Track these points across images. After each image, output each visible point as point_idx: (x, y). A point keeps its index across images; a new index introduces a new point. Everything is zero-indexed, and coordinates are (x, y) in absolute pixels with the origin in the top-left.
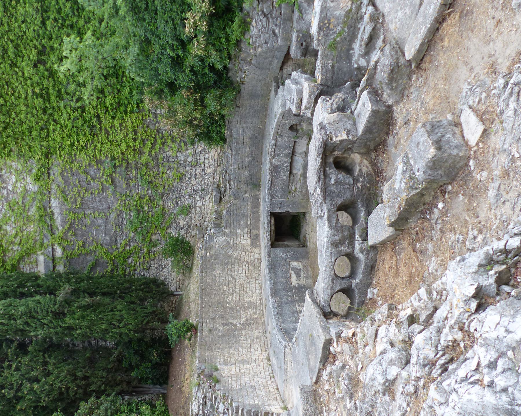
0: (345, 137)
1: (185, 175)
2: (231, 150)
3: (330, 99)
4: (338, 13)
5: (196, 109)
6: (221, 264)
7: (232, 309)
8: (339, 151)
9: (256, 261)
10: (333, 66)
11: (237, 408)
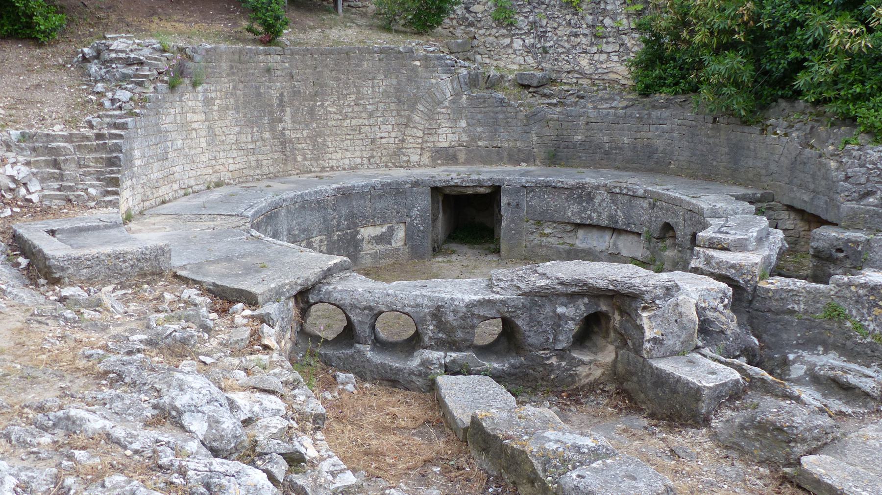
0: (648, 334)
1: (575, 14)
2: (626, 107)
3: (725, 306)
5: (712, 33)
6: (398, 90)
7: (312, 111)
8: (621, 322)
9: (406, 158)
10: (792, 312)
11: (124, 126)
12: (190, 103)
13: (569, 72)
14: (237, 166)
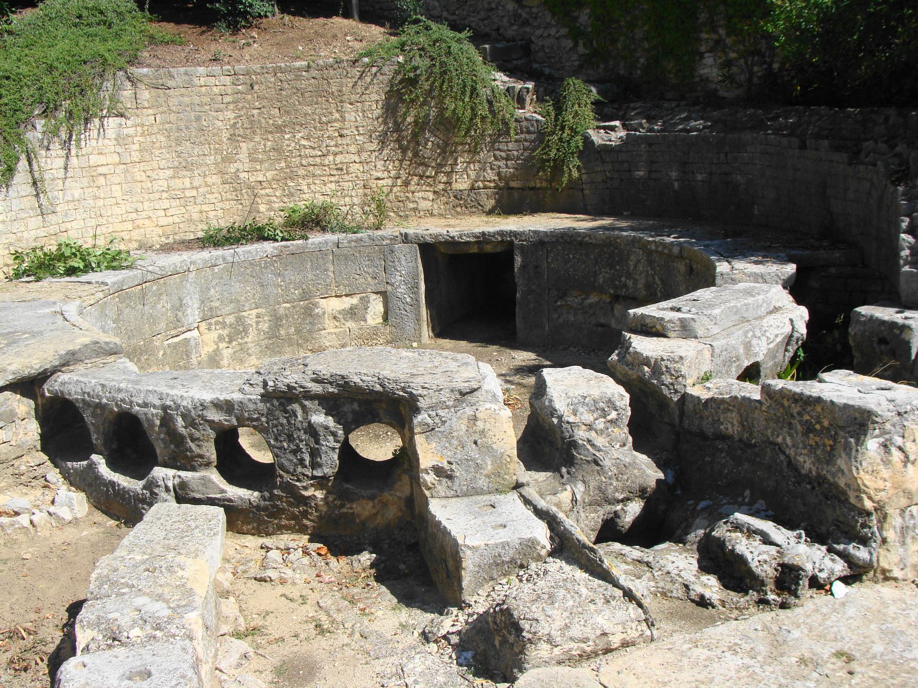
9: (412, 205)
14: (170, 220)
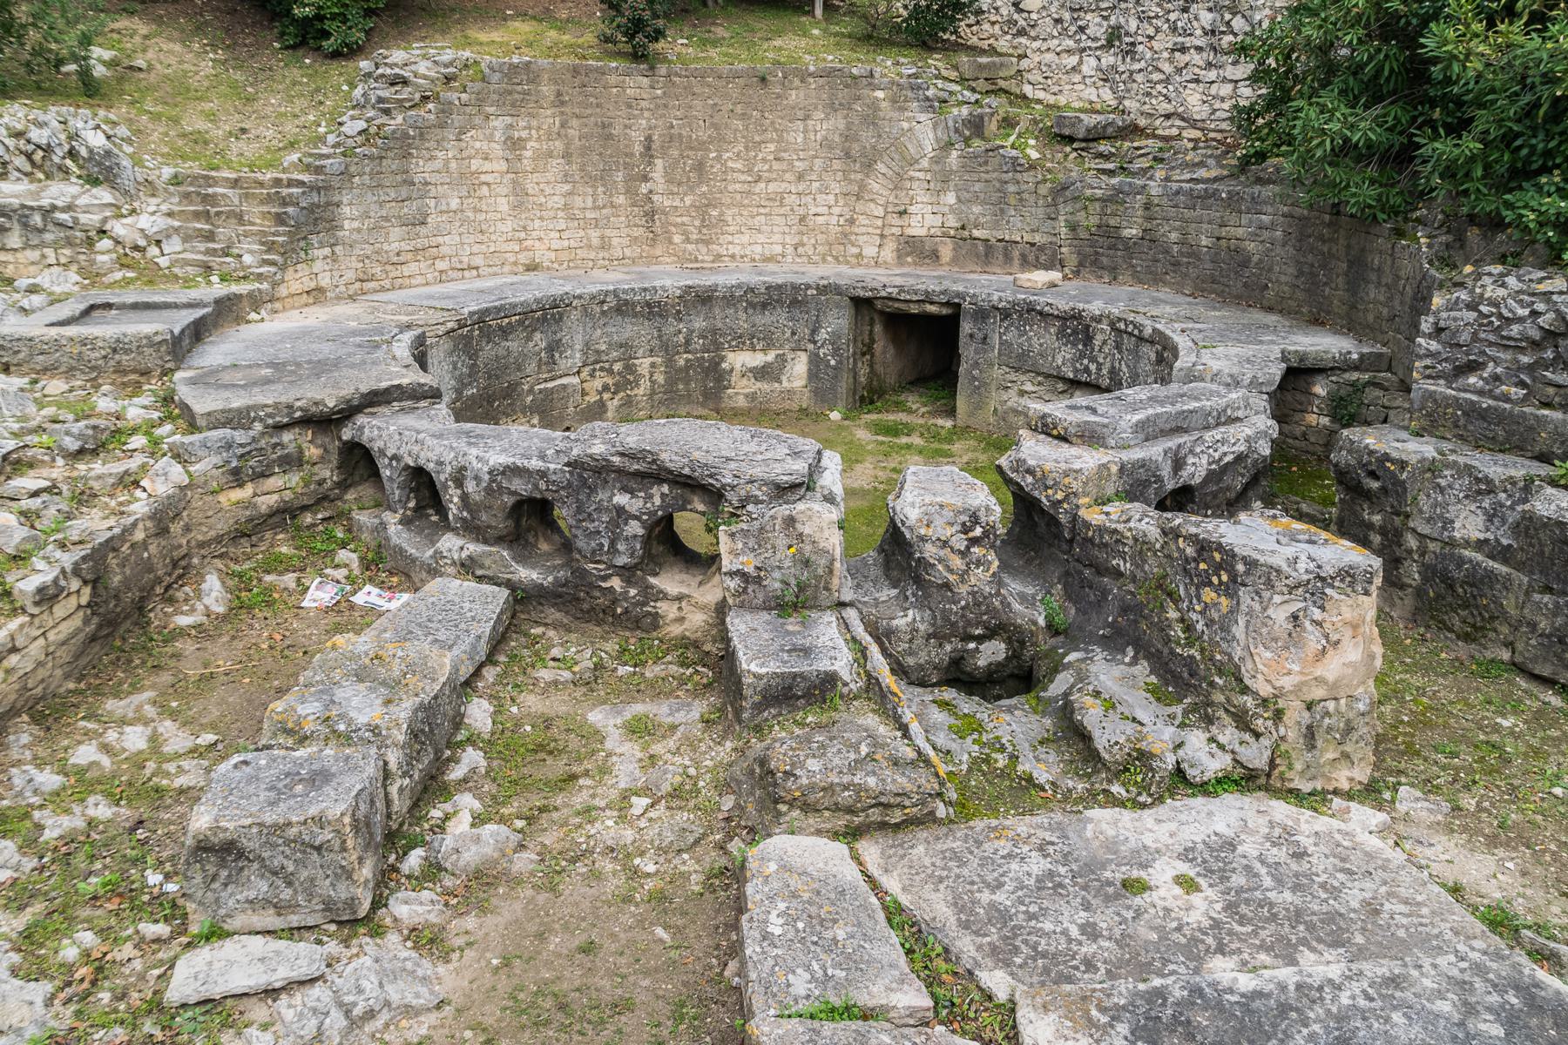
4: (1239, 630)
7: (700, 167)
9: (855, 250)
10: (1118, 574)
12: (478, 145)
13: (1168, 117)
14: (566, 243)
